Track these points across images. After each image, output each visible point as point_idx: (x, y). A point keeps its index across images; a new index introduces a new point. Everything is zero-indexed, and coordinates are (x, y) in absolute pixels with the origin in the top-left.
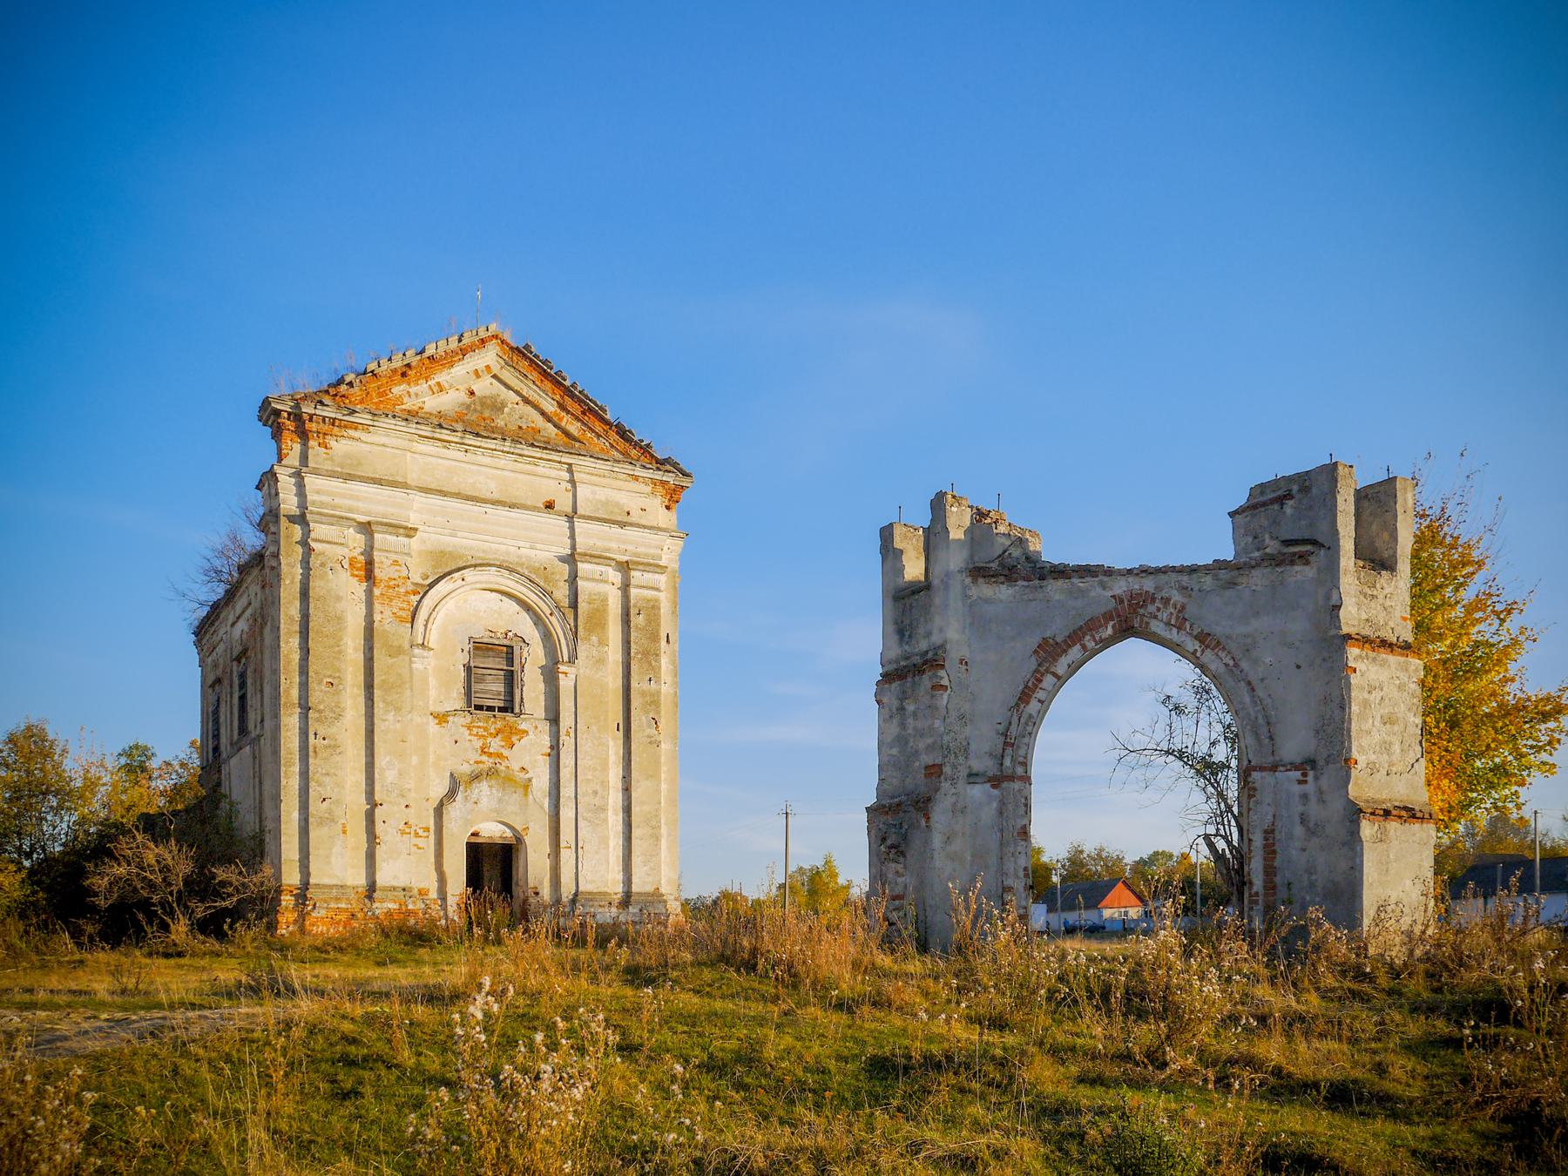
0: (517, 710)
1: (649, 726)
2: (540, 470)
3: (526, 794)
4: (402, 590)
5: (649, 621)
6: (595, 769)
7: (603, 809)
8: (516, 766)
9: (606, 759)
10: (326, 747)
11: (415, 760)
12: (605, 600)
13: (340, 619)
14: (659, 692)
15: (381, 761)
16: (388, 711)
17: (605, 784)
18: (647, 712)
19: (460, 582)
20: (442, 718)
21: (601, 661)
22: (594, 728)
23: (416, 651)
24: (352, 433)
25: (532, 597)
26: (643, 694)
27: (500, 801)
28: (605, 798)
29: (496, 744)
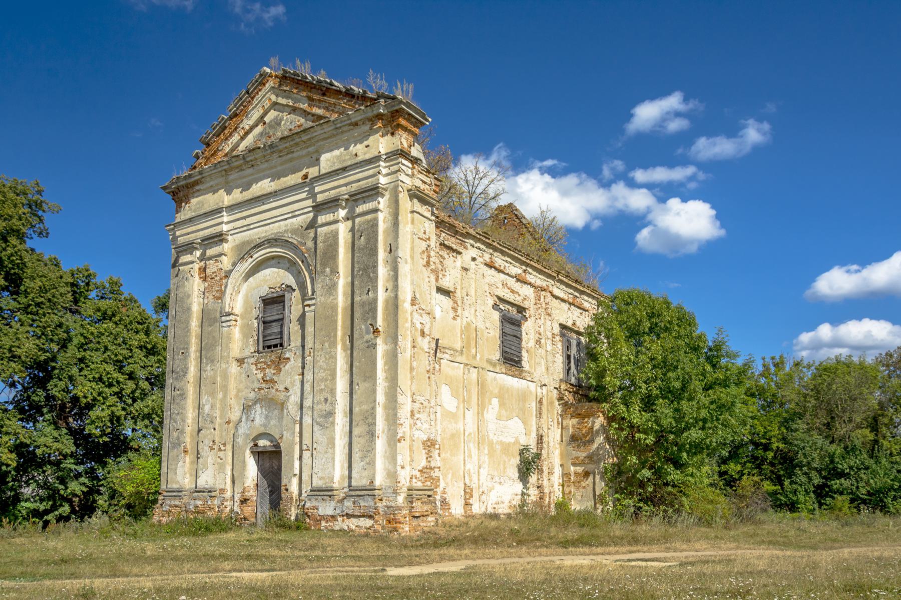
0: (285, 344)
1: (368, 332)
2: (295, 155)
3: (282, 410)
4: (218, 278)
5: (368, 240)
6: (326, 380)
7: (331, 414)
8: (282, 388)
9: (335, 370)
10: (179, 395)
11: (220, 395)
12: (335, 235)
13: (188, 310)
14: (375, 300)
15: (204, 399)
16: (207, 364)
17: (333, 391)
18: (365, 320)
19: (250, 260)
20: (241, 361)
21: (333, 287)
22: (326, 344)
23: (224, 319)
24: (197, 188)
25: (290, 255)
26: (363, 304)
27: (267, 417)
28: (333, 404)
29: (270, 372)
